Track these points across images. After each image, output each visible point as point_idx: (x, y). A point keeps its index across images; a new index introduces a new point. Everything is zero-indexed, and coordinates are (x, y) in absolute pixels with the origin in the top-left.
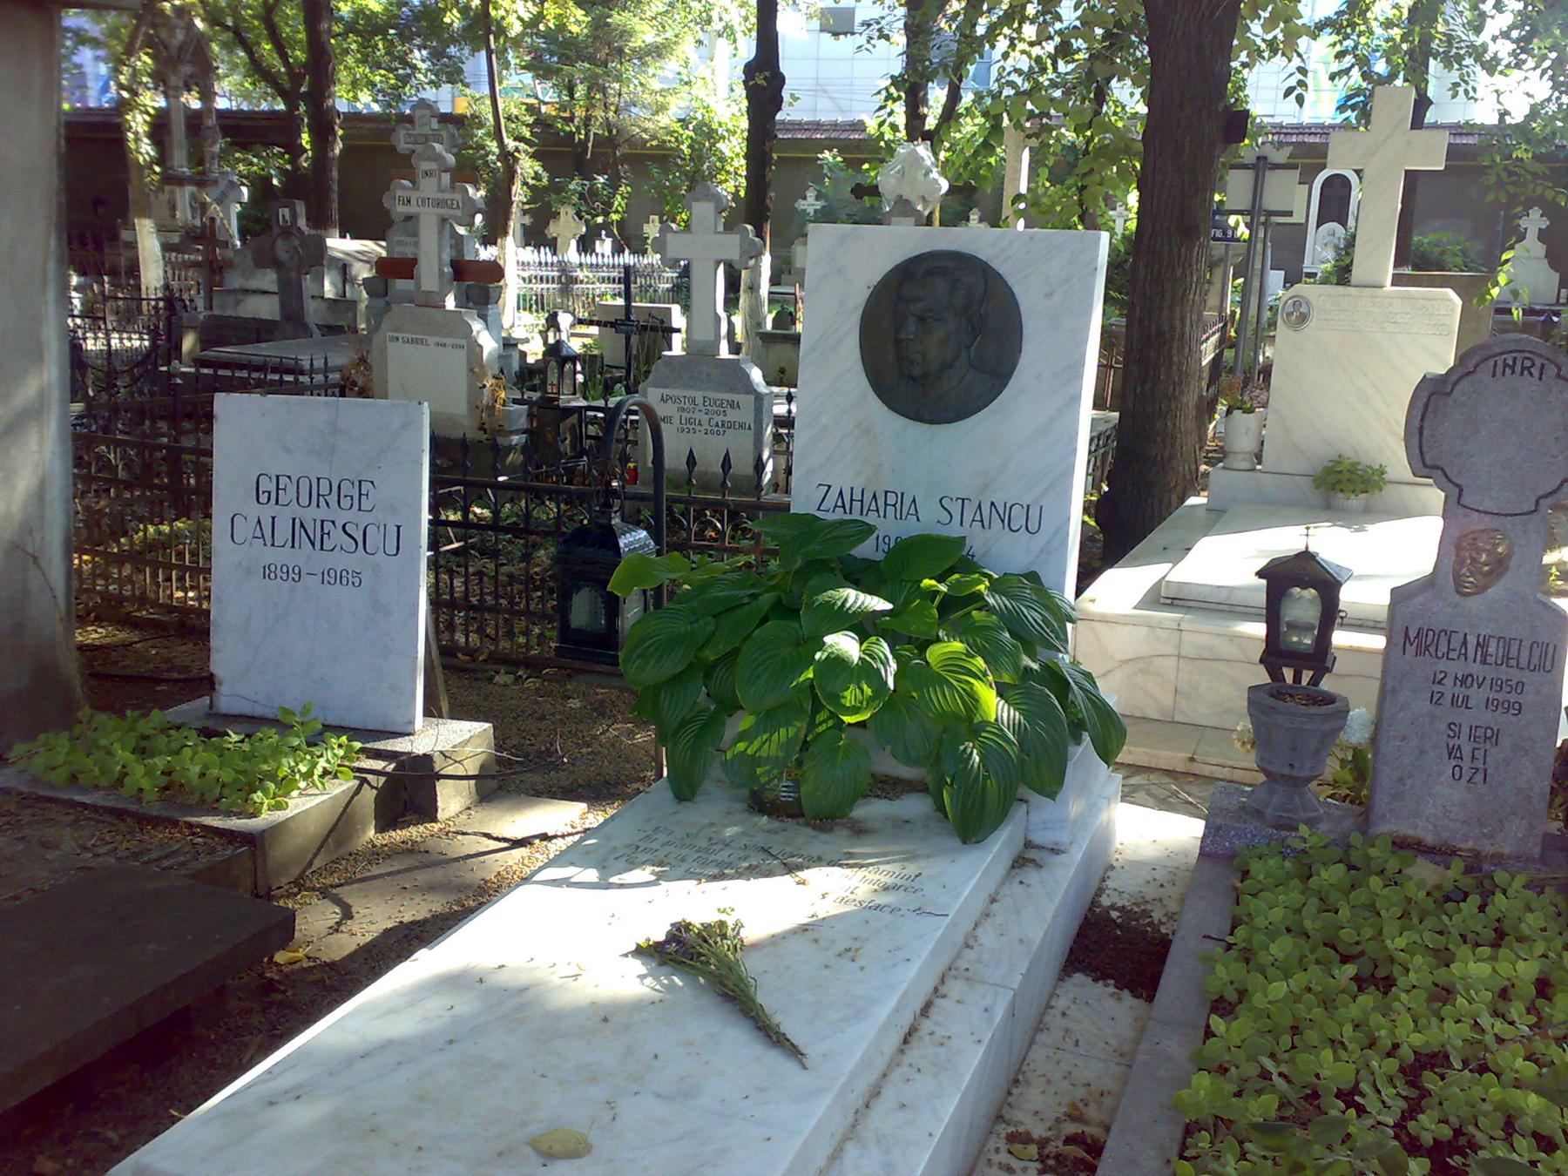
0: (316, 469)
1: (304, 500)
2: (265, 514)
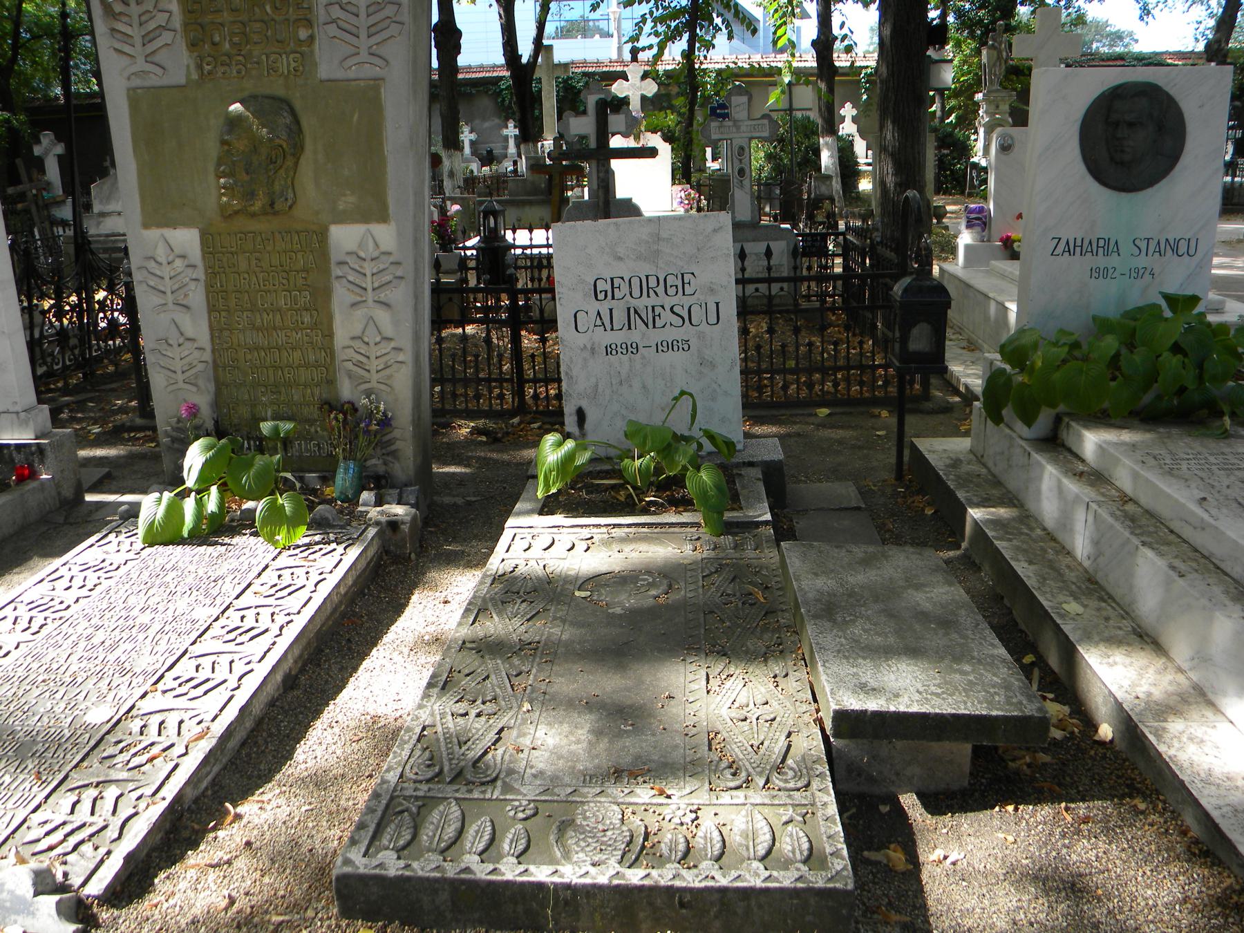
0: (644, 269)
1: (636, 293)
2: (604, 308)
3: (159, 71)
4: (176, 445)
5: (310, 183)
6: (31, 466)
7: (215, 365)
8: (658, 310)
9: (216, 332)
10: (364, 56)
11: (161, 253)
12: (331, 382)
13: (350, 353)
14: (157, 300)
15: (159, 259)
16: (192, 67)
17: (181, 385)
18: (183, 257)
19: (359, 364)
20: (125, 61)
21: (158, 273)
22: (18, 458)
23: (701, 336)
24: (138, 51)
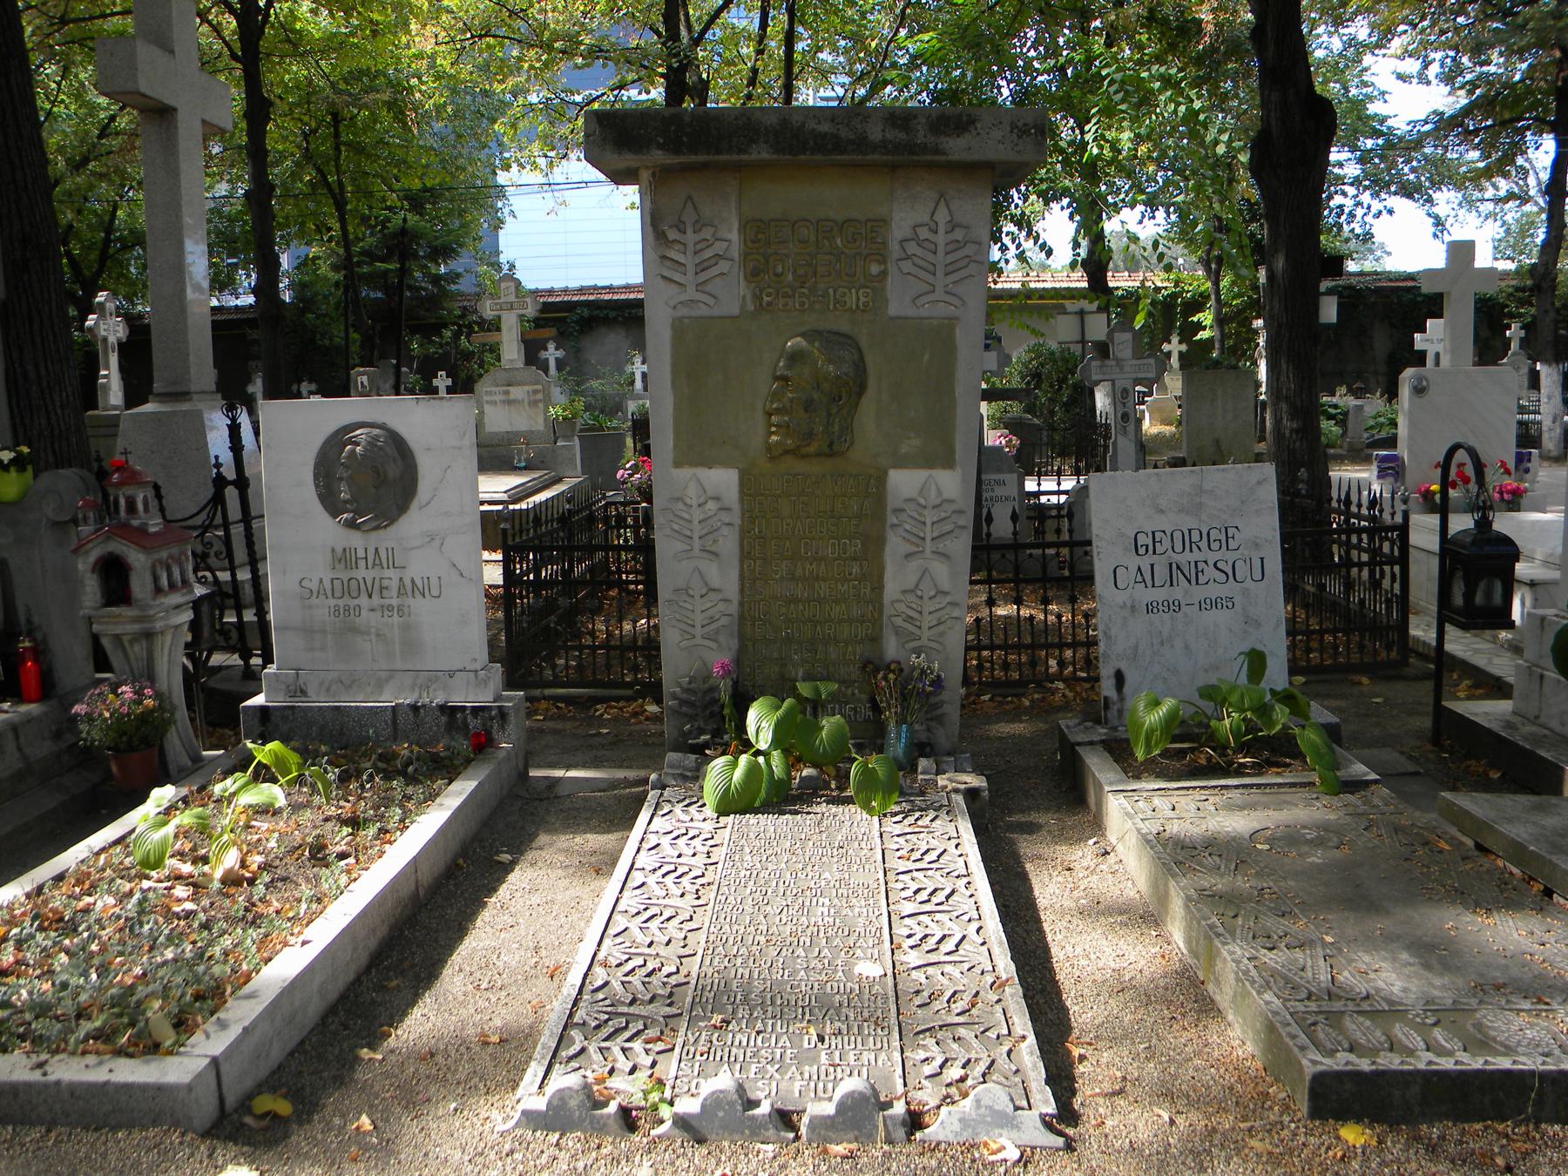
0: (1188, 522)
1: (1179, 548)
2: (1145, 563)
3: (711, 301)
4: (684, 709)
5: (870, 422)
6: (488, 733)
7: (742, 617)
8: (1201, 566)
9: (747, 582)
10: (939, 294)
11: (692, 494)
12: (876, 639)
13: (901, 607)
14: (679, 546)
15: (688, 501)
16: (749, 297)
17: (699, 641)
18: (717, 499)
19: (909, 619)
20: (672, 290)
21: (686, 516)
22: (474, 724)
23: (1246, 593)
24: (689, 279)
